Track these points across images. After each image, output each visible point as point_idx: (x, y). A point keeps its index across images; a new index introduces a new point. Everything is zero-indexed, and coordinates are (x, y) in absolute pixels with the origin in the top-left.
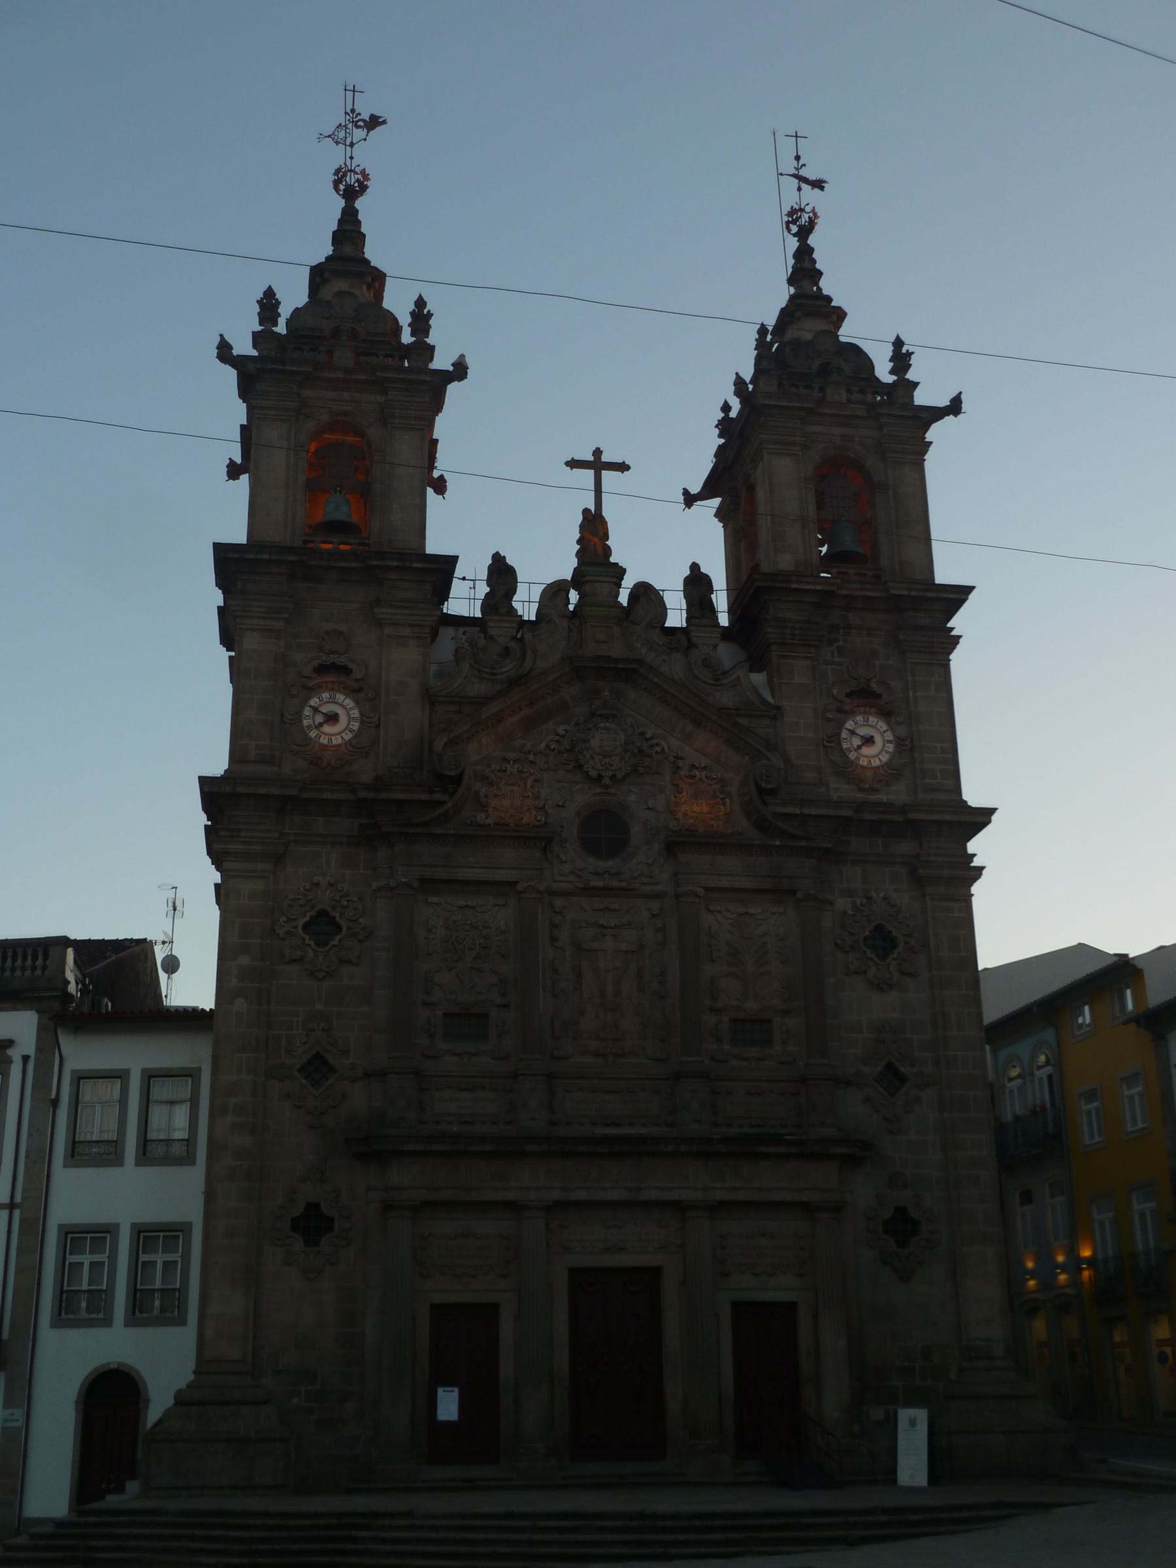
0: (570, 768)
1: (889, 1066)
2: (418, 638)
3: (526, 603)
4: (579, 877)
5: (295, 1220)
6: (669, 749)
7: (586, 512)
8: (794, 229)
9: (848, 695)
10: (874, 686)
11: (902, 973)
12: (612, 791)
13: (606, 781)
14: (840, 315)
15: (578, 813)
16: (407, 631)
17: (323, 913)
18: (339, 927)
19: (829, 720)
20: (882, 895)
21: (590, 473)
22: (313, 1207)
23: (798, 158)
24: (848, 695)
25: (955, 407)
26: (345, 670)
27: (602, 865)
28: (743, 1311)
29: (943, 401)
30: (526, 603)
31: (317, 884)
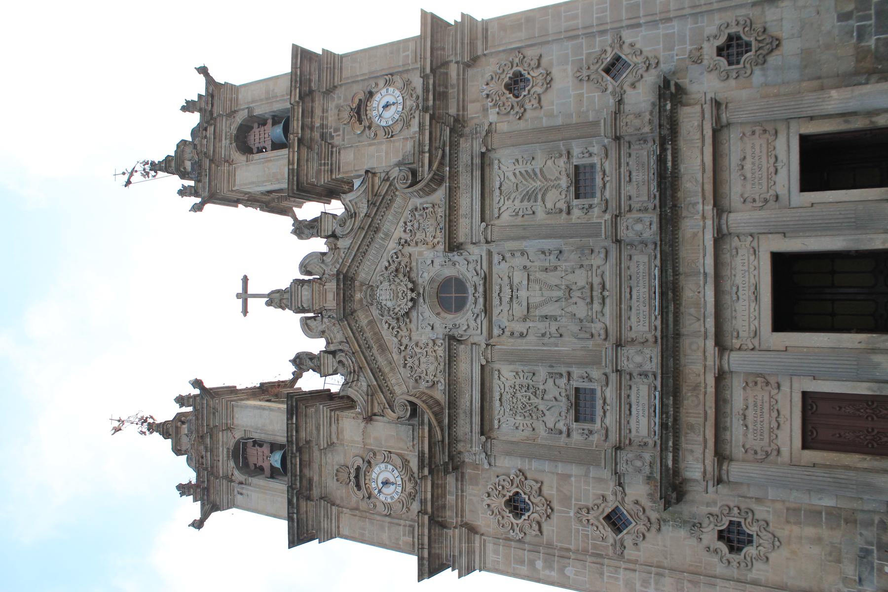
0: (408, 321)
1: (607, 71)
2: (338, 420)
3: (317, 346)
5: (732, 549)
7: (268, 304)
8: (152, 173)
10: (354, 106)
12: (421, 292)
13: (414, 295)
14: (184, 142)
15: (438, 314)
16: (334, 427)
18: (517, 493)
19: (376, 135)
20: (485, 87)
21: (249, 299)
22: (721, 536)
25: (203, 70)
26: (358, 469)
27: (471, 299)
29: (202, 79)
30: (317, 346)
31: (489, 505)
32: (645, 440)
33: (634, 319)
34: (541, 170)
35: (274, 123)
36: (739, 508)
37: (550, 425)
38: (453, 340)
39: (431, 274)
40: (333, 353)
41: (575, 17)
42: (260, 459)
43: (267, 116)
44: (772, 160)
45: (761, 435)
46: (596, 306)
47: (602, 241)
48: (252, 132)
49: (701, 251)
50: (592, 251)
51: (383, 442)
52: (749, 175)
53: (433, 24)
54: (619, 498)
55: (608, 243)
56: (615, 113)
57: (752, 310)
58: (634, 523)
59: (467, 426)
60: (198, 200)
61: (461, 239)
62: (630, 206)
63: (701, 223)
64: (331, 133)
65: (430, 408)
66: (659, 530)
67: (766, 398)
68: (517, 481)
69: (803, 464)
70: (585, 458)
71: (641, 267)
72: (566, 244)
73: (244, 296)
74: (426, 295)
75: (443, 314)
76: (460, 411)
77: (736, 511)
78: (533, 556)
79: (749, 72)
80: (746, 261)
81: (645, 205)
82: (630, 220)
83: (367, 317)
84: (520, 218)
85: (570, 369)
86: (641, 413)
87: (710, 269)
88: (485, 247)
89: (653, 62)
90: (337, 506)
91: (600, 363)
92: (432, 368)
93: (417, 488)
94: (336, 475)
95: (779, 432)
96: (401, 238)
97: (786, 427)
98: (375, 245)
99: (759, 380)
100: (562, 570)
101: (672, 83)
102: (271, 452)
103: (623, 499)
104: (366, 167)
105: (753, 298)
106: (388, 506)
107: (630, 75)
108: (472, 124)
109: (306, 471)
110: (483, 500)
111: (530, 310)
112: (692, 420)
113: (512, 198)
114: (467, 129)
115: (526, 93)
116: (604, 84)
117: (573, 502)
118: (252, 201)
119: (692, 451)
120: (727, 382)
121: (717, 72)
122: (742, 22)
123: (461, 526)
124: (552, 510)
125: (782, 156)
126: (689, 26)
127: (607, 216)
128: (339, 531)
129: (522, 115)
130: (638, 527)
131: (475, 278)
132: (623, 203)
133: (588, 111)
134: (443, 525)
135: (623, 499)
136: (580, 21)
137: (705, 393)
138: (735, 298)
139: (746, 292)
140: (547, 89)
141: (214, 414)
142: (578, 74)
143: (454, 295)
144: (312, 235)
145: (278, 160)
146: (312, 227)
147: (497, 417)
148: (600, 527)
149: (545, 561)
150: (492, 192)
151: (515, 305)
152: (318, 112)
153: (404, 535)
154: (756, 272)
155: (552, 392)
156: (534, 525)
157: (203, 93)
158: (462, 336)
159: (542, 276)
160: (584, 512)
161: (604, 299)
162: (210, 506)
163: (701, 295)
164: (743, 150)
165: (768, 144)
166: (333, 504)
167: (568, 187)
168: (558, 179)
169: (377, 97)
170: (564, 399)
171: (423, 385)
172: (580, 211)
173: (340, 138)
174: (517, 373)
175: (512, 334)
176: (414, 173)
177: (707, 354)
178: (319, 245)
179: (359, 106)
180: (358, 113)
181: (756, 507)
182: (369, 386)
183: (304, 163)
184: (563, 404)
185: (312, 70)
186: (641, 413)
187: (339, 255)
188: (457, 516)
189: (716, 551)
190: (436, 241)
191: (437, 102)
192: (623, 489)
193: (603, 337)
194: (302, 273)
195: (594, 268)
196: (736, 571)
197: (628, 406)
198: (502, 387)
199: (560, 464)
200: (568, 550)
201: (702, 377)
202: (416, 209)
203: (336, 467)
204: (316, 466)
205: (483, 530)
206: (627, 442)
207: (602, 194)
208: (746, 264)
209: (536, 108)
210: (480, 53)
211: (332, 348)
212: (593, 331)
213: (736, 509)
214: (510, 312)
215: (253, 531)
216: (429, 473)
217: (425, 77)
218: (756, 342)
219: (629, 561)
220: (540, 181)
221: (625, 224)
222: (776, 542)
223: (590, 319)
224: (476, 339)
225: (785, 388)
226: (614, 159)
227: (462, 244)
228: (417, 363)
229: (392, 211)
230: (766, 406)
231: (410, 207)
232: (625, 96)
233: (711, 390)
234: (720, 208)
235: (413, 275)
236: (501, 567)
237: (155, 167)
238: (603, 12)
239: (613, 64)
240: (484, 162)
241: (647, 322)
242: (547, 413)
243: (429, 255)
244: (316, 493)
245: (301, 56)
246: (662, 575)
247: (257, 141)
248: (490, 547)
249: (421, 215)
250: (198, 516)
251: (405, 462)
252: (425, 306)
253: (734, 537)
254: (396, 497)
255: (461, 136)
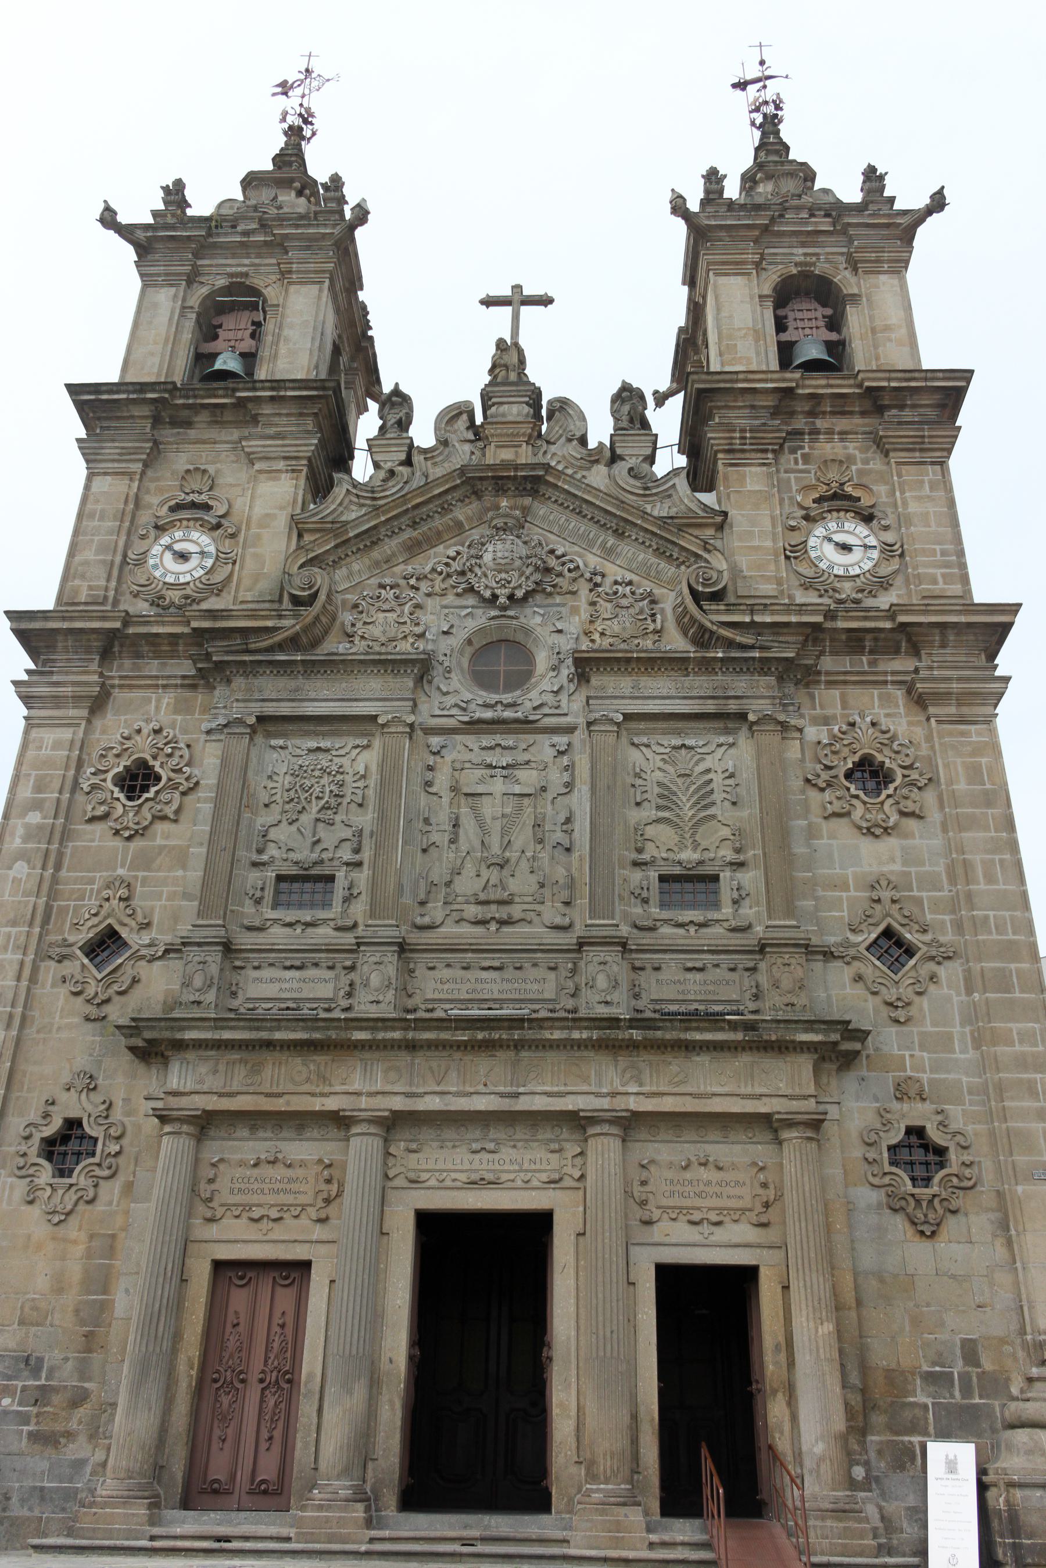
0: (459, 590)
1: (888, 933)
2: (293, 471)
3: (423, 433)
4: (464, 710)
6: (586, 565)
8: (759, 119)
9: (814, 501)
10: (848, 489)
11: (903, 814)
15: (469, 642)
16: (281, 465)
17: (143, 764)
18: (158, 778)
19: (793, 529)
20: (868, 719)
21: (508, 310)
22: (73, 1124)
23: (762, 63)
24: (814, 501)
25: (938, 203)
26: (207, 507)
27: (493, 698)
28: (672, 1280)
29: (921, 202)
30: (423, 433)
31: (139, 731)
32: (240, 993)
33: (447, 973)
34: (713, 817)
35: (831, 347)
36: (118, 1154)
37: (273, 834)
38: (422, 669)
39: (539, 629)
40: (408, 462)
41: (990, 879)
42: (231, 335)
43: (844, 330)
44: (714, 1218)
45: (240, 1190)
46: (473, 911)
47: (582, 920)
48: (815, 305)
49: (556, 1089)
50: (567, 904)
51: (251, 550)
52: (688, 1175)
53: (993, 628)
54: (143, 952)
55: (579, 930)
56: (807, 946)
57: (454, 1175)
58: (99, 977)
59: (274, 694)
60: (694, 206)
61: (595, 681)
62: (642, 969)
63: (605, 1090)
64: (802, 448)
65: (306, 629)
66: (87, 1019)
67: (302, 1199)
68: (180, 779)
69: (187, 1261)
70: (216, 892)
71: (535, 987)
72: (581, 859)
73: (517, 298)
74: (503, 621)
75: (469, 651)
76: (300, 681)
77: (114, 1148)
78: (50, 807)
79: (876, 1181)
80: (538, 1167)
81: (644, 995)
82: (615, 968)
83: (469, 519)
84: (630, 780)
85: (366, 866)
86: (287, 986)
87: (523, 1104)
88: (581, 721)
89: (901, 1015)
90: (143, 473)
91: (372, 915)
92: (376, 631)
93: (172, 610)
94: (197, 469)
95: (244, 1221)
96: (603, 576)
97: (253, 1232)
98: (594, 531)
99: (334, 1187)
100: (22, 855)
101: (857, 1046)
102: (242, 355)
103: (142, 957)
104: (732, 513)
105: (475, 1177)
106: (141, 560)
107: (878, 973)
108: (801, 696)
109: (204, 417)
110: (148, 721)
111: (470, 799)
112: (268, 1072)
113: (667, 767)
114: (792, 689)
115: (853, 791)
116: (863, 927)
117: (140, 874)
118: (696, 310)
119: (216, 1072)
120: (334, 1132)
121: (879, 1126)
122: (967, 1172)
123: (103, 685)
124: (129, 838)
125: (719, 1235)
126: (964, 1079)
127: (625, 930)
128: (98, 474)
129: (815, 785)
130: (93, 983)
131: (528, 705)
132: (648, 956)
133: (816, 899)
134: (106, 654)
135: (142, 957)
136: (982, 886)
137: (313, 1095)
138: (475, 1146)
139: (484, 1166)
140: (860, 828)
141: (308, 248)
142: (884, 883)
143: (502, 668)
144: (617, 420)
145: (758, 354)
146: (631, 421)
147: (289, 743)
148: (95, 920)
149: (40, 827)
150: (678, 733)
151: (479, 773)
152: (842, 424)
153: (90, 588)
154: (519, 1183)
155: (329, 837)
156: (101, 810)
157: (898, 206)
158: (430, 682)
159: (528, 818)
160: (123, 892)
161: (483, 922)
162: (145, 242)
163: (481, 1088)
164: (734, 1167)
165: (743, 1210)
166: (146, 465)
167: (680, 863)
168: (696, 845)
169: (862, 530)
170: (314, 856)
171: (347, 617)
172: (637, 883)
173: (792, 465)
174: (364, 777)
175: (430, 768)
176: (717, 597)
177: (379, 1097)
178: (600, 430)
179: (849, 498)
180: (835, 496)
181: (117, 1184)
182: (347, 522)
183: (749, 400)
184: (304, 854)
185: (922, 410)
186: (287, 986)
187: (581, 468)
188: (121, 677)
189: (46, 1115)
190: (596, 636)
191: (844, 637)
192: (160, 958)
193: (419, 921)
194: (550, 402)
195: (537, 907)
196: (13, 1149)
197: (298, 963)
198: (342, 752)
199: (204, 850)
200: (58, 867)
201: (338, 1088)
202: (653, 602)
203: (211, 469)
204: (213, 433)
205: (98, 723)
206: (238, 963)
207: (665, 921)
208: (533, 1167)
209: (825, 808)
210: (932, 710)
211: (417, 459)
212: (430, 905)
213: (117, 1148)
214: (467, 765)
215: (101, 319)
216: (194, 629)
217: (891, 613)
218: (399, 1182)
219: (35, 969)
220: (693, 816)
221: (608, 958)
222: (60, 1218)
223: (450, 899)
224: (424, 707)
225: (318, 1232)
226: (725, 942)
227: (588, 681)
228: (385, 607)
229: (654, 560)
230: (289, 1199)
231: (657, 591)
232: (838, 964)
233: (318, 1105)
234: (631, 1124)
235: (539, 598)
236: (31, 753)
237: (770, 127)
238: (997, 928)
239: (899, 943)
240: (730, 719)
241: (442, 996)
242: (293, 828)
243: (574, 625)
244: (168, 434)
245: (949, 392)
246: (8, 1026)
247: (799, 315)
248: (66, 734)
249: (641, 612)
250: (123, 219)
251: (218, 589)
252: (484, 620)
253: (73, 1146)
254: (157, 574)
255: (780, 679)
